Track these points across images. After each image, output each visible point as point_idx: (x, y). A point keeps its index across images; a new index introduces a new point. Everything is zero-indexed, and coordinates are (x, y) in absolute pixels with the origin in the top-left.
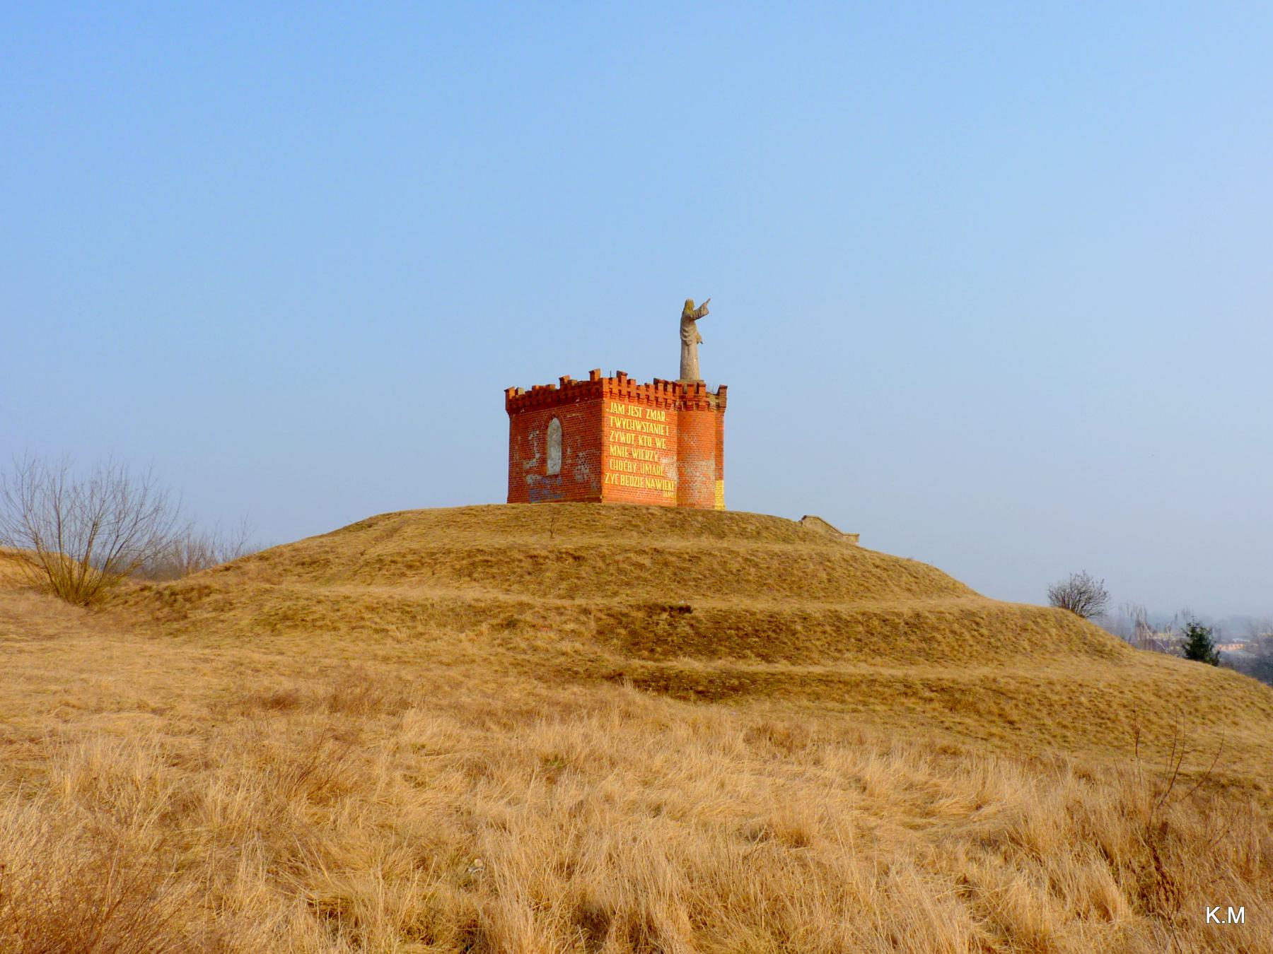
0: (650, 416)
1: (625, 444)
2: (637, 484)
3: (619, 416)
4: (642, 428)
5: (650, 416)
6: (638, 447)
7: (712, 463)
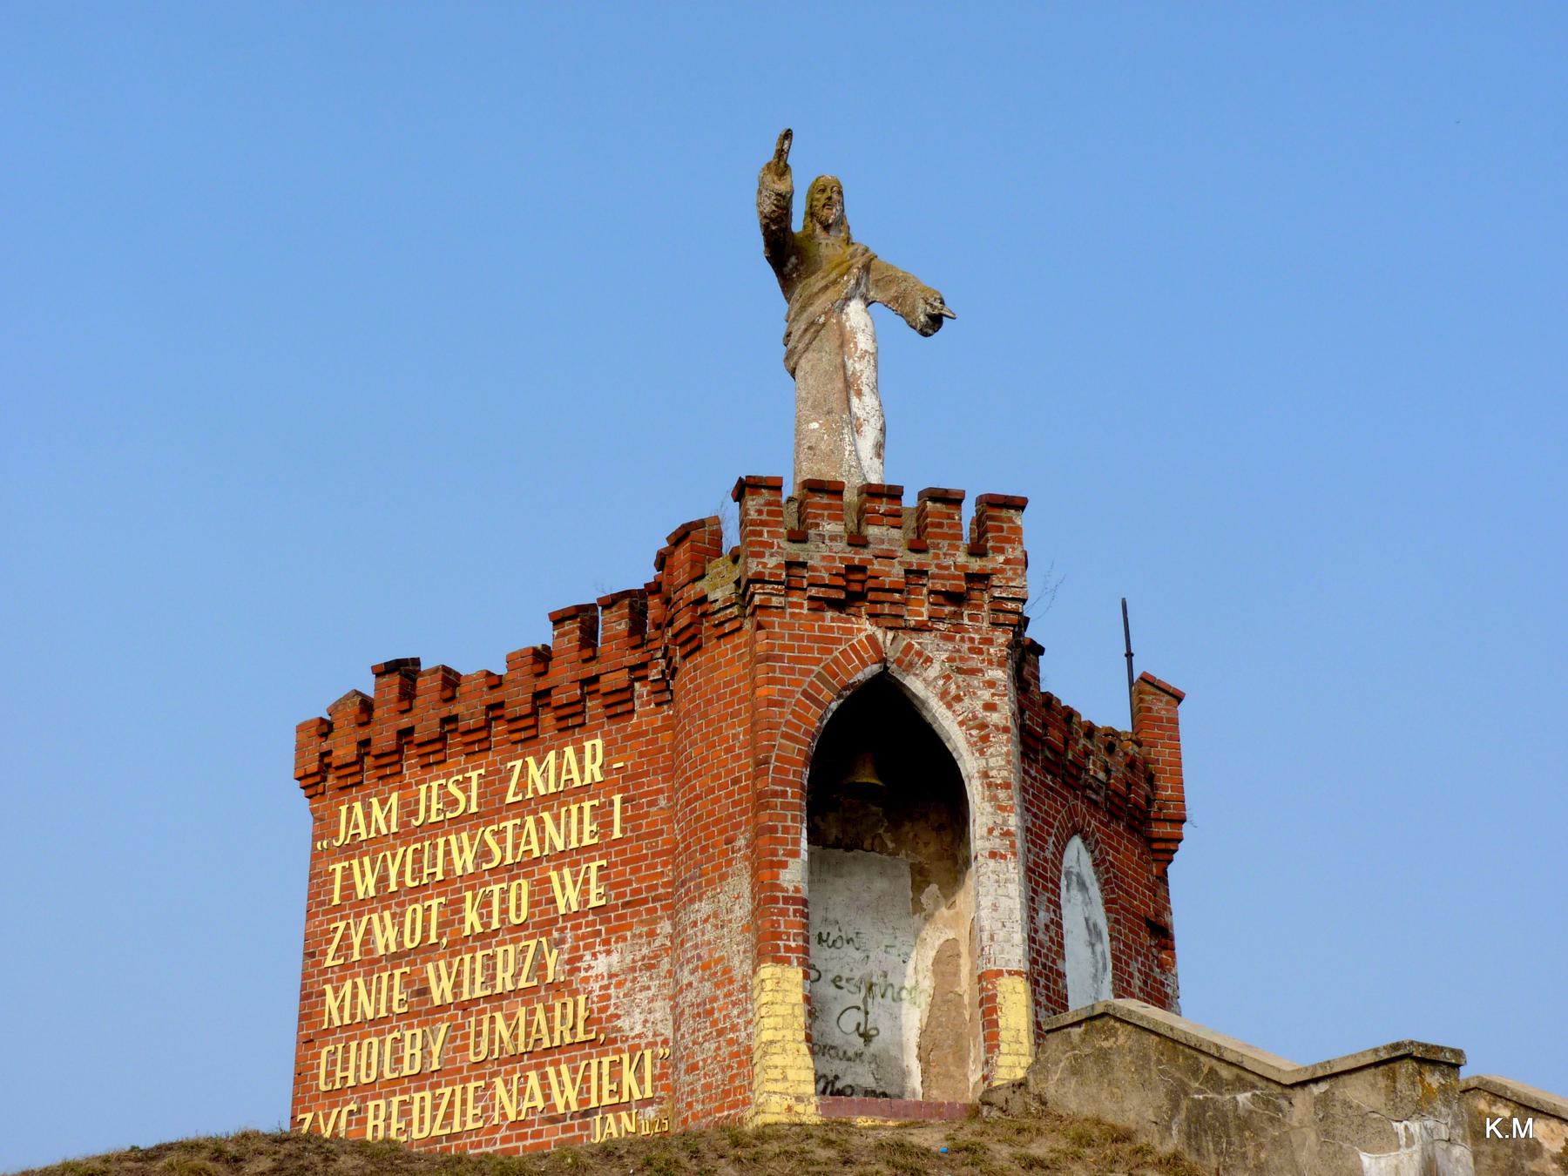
0: (522, 786)
2: (449, 1116)
3: (378, 843)
4: (484, 854)
5: (522, 786)
6: (458, 945)
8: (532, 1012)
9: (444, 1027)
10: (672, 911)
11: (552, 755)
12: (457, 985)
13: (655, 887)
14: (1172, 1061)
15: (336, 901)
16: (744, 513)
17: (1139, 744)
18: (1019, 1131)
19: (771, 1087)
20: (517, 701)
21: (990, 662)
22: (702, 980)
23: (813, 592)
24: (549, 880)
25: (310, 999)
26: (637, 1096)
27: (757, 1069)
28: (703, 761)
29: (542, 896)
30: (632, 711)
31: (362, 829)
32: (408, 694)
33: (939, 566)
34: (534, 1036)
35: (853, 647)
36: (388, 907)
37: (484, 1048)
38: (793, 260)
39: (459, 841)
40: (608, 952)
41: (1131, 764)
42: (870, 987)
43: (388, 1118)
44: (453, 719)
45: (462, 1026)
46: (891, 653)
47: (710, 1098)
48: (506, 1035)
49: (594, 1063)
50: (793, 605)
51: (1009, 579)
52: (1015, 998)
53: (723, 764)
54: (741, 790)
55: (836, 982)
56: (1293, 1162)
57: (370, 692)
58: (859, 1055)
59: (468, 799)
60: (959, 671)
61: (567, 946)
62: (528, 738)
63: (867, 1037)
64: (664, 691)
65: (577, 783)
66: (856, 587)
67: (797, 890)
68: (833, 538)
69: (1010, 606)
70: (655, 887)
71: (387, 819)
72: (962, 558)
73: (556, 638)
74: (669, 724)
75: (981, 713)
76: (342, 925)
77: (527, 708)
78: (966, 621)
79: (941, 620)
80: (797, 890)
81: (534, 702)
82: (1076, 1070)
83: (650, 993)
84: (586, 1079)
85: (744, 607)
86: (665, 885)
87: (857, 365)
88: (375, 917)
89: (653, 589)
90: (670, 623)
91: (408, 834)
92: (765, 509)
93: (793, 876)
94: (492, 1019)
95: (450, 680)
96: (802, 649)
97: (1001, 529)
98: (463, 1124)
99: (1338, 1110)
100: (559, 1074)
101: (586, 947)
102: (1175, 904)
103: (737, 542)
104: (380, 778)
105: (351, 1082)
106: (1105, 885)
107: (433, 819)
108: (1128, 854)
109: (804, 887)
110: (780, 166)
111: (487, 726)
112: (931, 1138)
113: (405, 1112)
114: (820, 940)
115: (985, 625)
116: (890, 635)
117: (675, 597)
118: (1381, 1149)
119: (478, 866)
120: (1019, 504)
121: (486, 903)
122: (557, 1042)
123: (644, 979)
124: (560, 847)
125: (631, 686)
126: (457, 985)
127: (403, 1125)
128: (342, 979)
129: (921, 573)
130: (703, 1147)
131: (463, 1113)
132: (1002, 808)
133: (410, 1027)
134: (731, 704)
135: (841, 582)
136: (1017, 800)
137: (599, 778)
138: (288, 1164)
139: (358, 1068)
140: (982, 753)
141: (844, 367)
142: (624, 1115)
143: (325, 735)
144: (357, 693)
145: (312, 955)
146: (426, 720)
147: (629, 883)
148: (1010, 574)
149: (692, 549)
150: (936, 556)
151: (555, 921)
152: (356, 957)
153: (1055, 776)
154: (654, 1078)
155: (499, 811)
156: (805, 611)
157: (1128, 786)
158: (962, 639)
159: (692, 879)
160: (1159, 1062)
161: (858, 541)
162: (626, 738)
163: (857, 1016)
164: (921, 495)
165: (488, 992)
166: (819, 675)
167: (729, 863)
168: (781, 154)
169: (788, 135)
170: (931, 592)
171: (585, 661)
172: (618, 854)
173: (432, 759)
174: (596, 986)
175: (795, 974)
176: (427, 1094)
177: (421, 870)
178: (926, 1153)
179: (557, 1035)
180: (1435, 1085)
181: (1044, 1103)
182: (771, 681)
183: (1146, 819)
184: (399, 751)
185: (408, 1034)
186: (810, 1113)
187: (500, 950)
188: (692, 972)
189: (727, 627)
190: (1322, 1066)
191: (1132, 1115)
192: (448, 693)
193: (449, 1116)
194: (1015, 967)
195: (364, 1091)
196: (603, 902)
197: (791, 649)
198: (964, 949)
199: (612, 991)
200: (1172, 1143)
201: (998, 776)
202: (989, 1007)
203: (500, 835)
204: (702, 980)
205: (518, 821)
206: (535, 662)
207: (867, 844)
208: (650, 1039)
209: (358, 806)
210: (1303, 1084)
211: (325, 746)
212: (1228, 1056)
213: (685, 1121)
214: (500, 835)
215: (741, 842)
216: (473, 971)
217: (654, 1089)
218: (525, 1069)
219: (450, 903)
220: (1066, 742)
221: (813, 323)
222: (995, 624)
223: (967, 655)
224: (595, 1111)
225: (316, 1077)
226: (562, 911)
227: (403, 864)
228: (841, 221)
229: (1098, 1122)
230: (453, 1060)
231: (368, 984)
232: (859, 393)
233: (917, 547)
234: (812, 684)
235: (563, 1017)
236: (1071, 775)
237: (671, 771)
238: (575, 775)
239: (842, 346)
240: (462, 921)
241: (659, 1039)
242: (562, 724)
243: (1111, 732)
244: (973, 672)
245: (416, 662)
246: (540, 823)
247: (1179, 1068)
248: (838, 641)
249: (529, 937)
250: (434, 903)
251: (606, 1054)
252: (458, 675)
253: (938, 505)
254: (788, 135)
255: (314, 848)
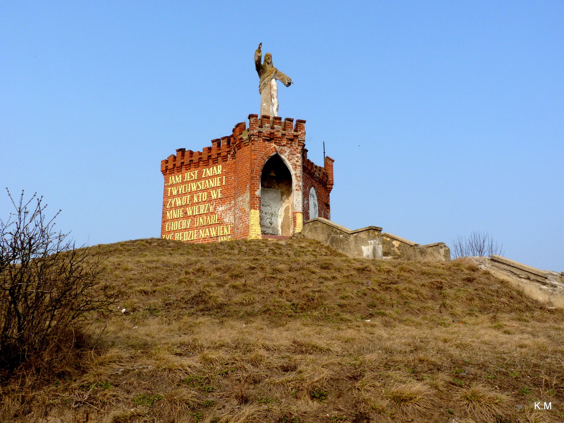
0: (205, 174)
1: (181, 206)
2: (191, 236)
3: (177, 184)
4: (198, 187)
5: (205, 174)
6: (193, 204)
7: (247, 196)
8: (207, 218)
9: (190, 220)
10: (234, 199)
11: (211, 168)
12: (193, 212)
13: (231, 194)
14: (329, 229)
15: (169, 195)
16: (250, 121)
17: (325, 170)
18: (299, 241)
19: (253, 233)
20: (205, 157)
21: (298, 153)
22: (240, 212)
23: (263, 138)
24: (210, 192)
25: (164, 214)
26: (227, 234)
27: (250, 229)
28: (241, 170)
29: (209, 195)
30: (227, 160)
31: (174, 182)
32: (183, 155)
33: (288, 134)
34: (207, 222)
35: (271, 149)
36: (179, 197)
37: (198, 224)
38: (261, 70)
39: (193, 184)
40: (222, 207)
41: (324, 174)
42: (272, 214)
43: (179, 236)
44: (192, 161)
45: (194, 220)
46: (278, 150)
47: (241, 234)
48: (202, 222)
49: (219, 227)
50: (259, 140)
51: (302, 137)
52: (300, 217)
53: (245, 171)
54: (248, 176)
55: (266, 213)
56: (350, 248)
57: (176, 155)
58: (270, 227)
59: (195, 176)
60: (291, 154)
61: (214, 205)
62: (207, 165)
63: (271, 224)
64: (234, 157)
65: (216, 174)
66: (272, 137)
67: (259, 195)
68: (268, 127)
69: (302, 142)
70: (231, 194)
71: (179, 180)
72: (293, 132)
73: (212, 145)
74: (234, 163)
75: (295, 162)
76: (170, 200)
77: (207, 159)
78: (293, 144)
79: (288, 144)
80: (259, 195)
81: (208, 158)
82: (310, 231)
83: (230, 215)
84: (217, 230)
85: (250, 140)
86: (233, 194)
87: (274, 93)
88: (177, 199)
89: (232, 136)
90: (235, 143)
91: (183, 183)
92: (254, 121)
93: (258, 193)
94: (199, 219)
95: (191, 153)
96: (261, 149)
97: (301, 127)
98: (194, 238)
99: (358, 238)
100: (212, 229)
101: (218, 205)
102: (330, 201)
103: (249, 127)
104: (178, 172)
105: (172, 230)
106: (318, 196)
107: (188, 180)
108: (322, 190)
109: (260, 195)
110: (259, 51)
111: (199, 162)
112: (283, 242)
113: (183, 236)
114: (263, 205)
115: (297, 145)
116: (278, 147)
117: (236, 138)
118: (366, 246)
119: (197, 189)
120: (304, 122)
121: (198, 197)
122: (212, 223)
123: (229, 212)
124: (213, 186)
125: (227, 155)
126: (193, 212)
127: (182, 238)
128: (170, 210)
129: (285, 135)
130: (239, 243)
131: (194, 236)
132: (299, 181)
133: (184, 220)
134: (247, 159)
135: (269, 136)
136: (301, 180)
137: (221, 173)
138: (160, 244)
139: (173, 227)
140: (295, 170)
141: (271, 93)
142: (224, 237)
143: (167, 163)
144: (173, 155)
145: (164, 205)
146: (187, 160)
147: (226, 193)
148: (302, 135)
149: (240, 128)
150: (288, 131)
151: (212, 200)
152: (173, 206)
153: (309, 175)
154: (230, 230)
155: (201, 179)
156: (262, 141)
157: (323, 178)
158: (292, 148)
159: (238, 193)
160: (326, 229)
161: (272, 128)
162: (226, 165)
163: (270, 220)
164: (285, 119)
165: (199, 213)
166: (264, 154)
167: (246, 190)
168: (259, 48)
169: (261, 44)
170: (286, 139)
171: (218, 150)
172: (224, 188)
173: (188, 168)
174: (219, 213)
175: (258, 211)
176: (187, 232)
177: (186, 190)
178: (282, 245)
179: (212, 222)
180: (376, 234)
181: (304, 237)
182: (255, 155)
183: (326, 184)
184: (181, 166)
185: (183, 221)
186: (260, 237)
187: (201, 206)
188: (238, 211)
189: (246, 144)
190: (356, 230)
191: (321, 239)
192: (191, 155)
193: (191, 236)
194: (300, 211)
195: (175, 231)
196: (221, 197)
197: (259, 149)
198: (290, 208)
199: (222, 214)
200: (328, 244)
201: (298, 175)
202: (295, 219)
203: (201, 184)
204: (240, 212)
205: (205, 181)
206: (208, 150)
207: (272, 187)
208: (230, 223)
209: (173, 177)
210: (352, 234)
211: (167, 165)
212: (339, 228)
213: (236, 238)
214: (201, 184)
215: (248, 186)
216: (196, 209)
217: (230, 233)
218: (206, 228)
219: (191, 196)
220: (311, 169)
221: (265, 83)
222: (299, 145)
223: (293, 151)
224: (219, 236)
225: (166, 229)
226: (213, 198)
227: (182, 189)
228: (271, 62)
229: (314, 240)
230: (192, 226)
231: (175, 211)
232: (274, 98)
233: (284, 130)
234: (263, 156)
235: (213, 218)
236: (312, 175)
237: (235, 172)
238: (216, 172)
239: (270, 88)
240: (194, 200)
241: (231, 223)
242: (214, 162)
243: (320, 167)
244: (294, 154)
245: (185, 149)
246: (209, 181)
247: (330, 230)
248: (268, 147)
249: (207, 203)
250: (188, 196)
251: (221, 226)
252: (193, 152)
253: (289, 121)
254: (261, 44)
255: (165, 185)
